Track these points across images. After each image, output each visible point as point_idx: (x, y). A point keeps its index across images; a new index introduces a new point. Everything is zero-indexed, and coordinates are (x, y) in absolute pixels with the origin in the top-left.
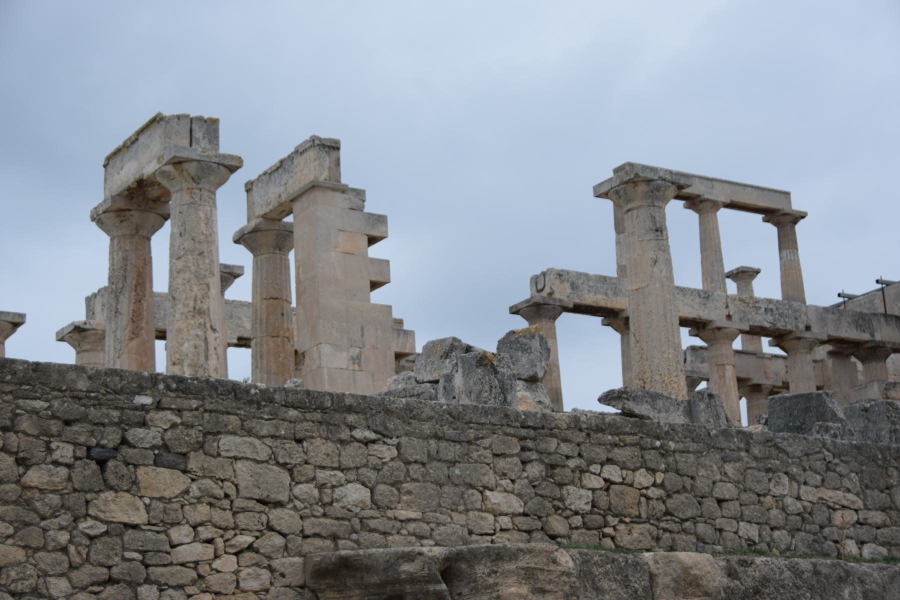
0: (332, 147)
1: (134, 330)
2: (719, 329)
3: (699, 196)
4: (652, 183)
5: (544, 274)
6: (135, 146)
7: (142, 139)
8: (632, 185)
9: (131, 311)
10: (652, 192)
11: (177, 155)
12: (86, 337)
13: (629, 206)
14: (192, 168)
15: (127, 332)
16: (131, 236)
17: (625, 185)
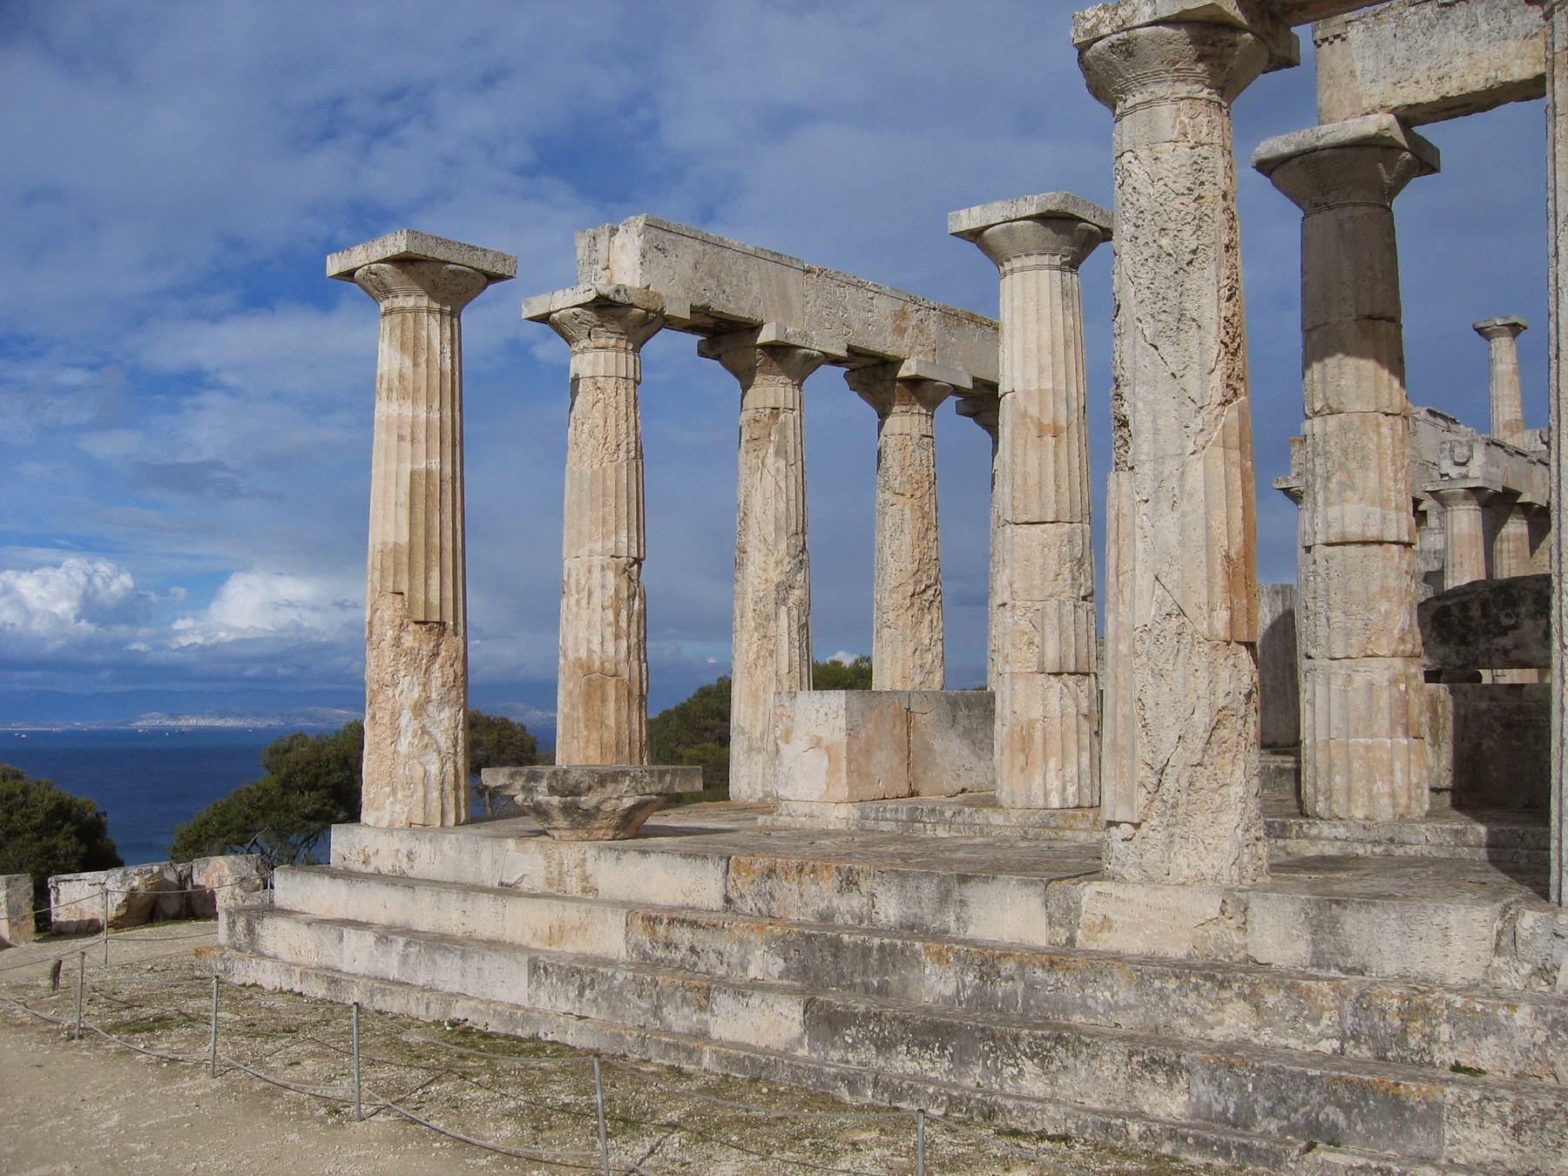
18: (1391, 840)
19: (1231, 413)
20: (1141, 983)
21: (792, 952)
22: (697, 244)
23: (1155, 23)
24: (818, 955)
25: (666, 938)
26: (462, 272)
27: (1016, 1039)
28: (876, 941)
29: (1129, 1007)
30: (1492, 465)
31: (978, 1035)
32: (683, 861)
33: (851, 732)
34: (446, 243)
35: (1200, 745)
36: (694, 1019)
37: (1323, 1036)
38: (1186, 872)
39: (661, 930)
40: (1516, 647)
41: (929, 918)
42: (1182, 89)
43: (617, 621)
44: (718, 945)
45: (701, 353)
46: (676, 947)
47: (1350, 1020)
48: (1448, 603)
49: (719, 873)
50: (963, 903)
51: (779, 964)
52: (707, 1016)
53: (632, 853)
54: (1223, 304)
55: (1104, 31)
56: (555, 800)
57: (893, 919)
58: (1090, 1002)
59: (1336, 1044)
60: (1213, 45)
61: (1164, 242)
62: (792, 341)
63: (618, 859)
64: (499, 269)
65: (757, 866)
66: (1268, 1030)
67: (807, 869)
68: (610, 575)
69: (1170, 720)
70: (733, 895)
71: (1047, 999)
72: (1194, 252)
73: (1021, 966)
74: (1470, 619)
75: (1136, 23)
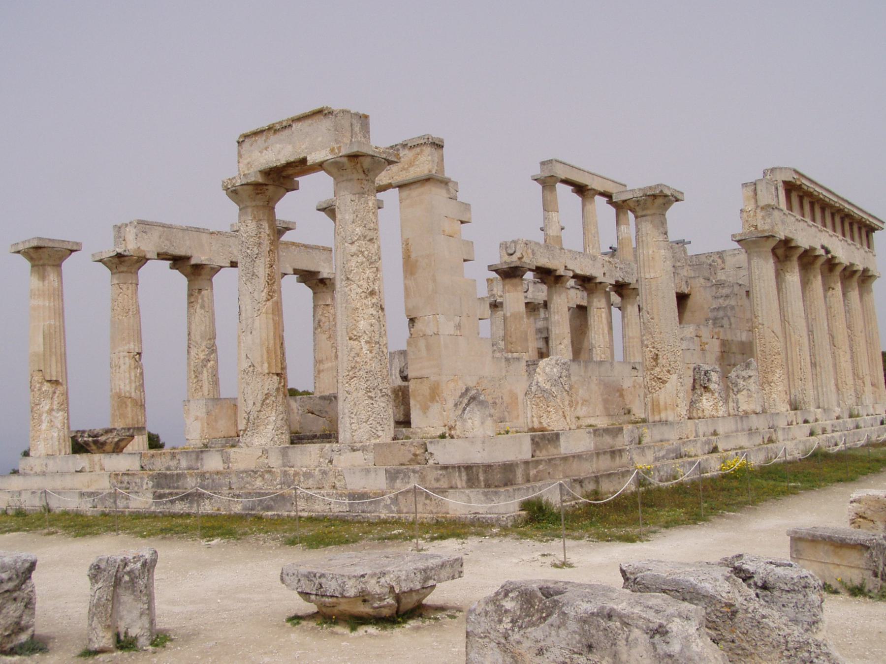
0: (438, 145)
1: (269, 292)
2: (600, 283)
3: (587, 185)
4: (667, 198)
5: (514, 242)
6: (287, 132)
7: (296, 126)
8: (653, 198)
9: (267, 275)
10: (664, 204)
11: (360, 150)
12: (124, 261)
13: (644, 213)
14: (367, 162)
15: (263, 294)
16: (264, 206)
17: (647, 197)
19: (269, 303)
22: (160, 228)
23: (242, 185)
26: (59, 251)
29: (235, 483)
30: (538, 292)
33: (208, 413)
34: (53, 240)
35: (260, 405)
36: (125, 503)
37: (278, 484)
38: (257, 443)
39: (119, 477)
42: (254, 204)
43: (130, 377)
45: (171, 268)
47: (283, 478)
49: (139, 458)
50: (202, 459)
51: (151, 484)
52: (128, 501)
54: (267, 270)
55: (229, 187)
56: (91, 439)
59: (280, 486)
60: (261, 190)
61: (248, 251)
62: (204, 263)
64: (75, 248)
66: (266, 484)
68: (127, 359)
69: (251, 397)
70: (143, 465)
72: (257, 254)
73: (211, 475)
75: (237, 185)
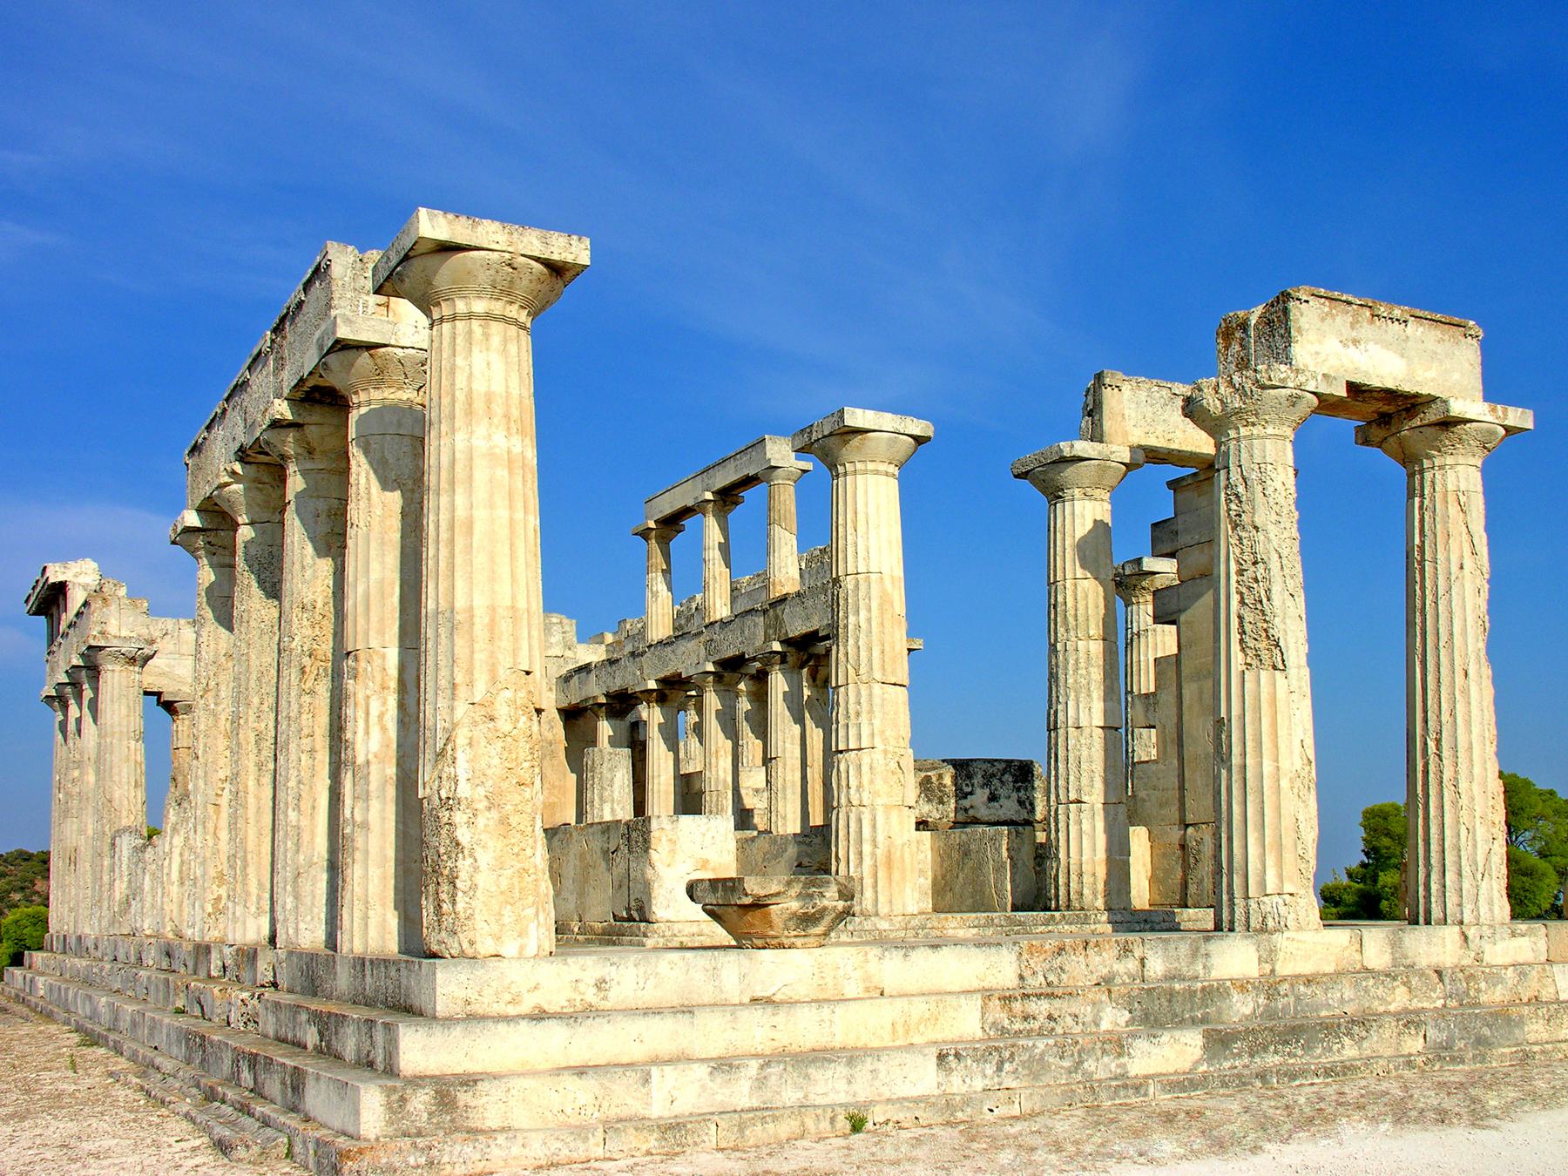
18: (1146, 921)
20: (1356, 985)
21: (1136, 1004)
24: (1157, 1002)
25: (1023, 1012)
27: (1339, 1026)
28: (1199, 985)
29: (1351, 1000)
31: (1318, 1028)
32: (977, 950)
39: (1017, 1006)
40: (972, 807)
41: (1185, 969)
44: (1073, 1010)
46: (1034, 1018)
48: (929, 774)
49: (1014, 957)
53: (923, 949)
57: (1160, 974)
58: (1331, 1002)
63: (906, 955)
65: (1047, 947)
67: (1091, 944)
70: (1027, 973)
71: (1307, 1005)
73: (1292, 986)
74: (945, 787)
